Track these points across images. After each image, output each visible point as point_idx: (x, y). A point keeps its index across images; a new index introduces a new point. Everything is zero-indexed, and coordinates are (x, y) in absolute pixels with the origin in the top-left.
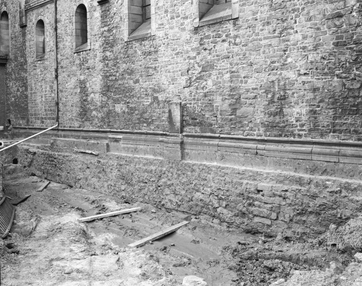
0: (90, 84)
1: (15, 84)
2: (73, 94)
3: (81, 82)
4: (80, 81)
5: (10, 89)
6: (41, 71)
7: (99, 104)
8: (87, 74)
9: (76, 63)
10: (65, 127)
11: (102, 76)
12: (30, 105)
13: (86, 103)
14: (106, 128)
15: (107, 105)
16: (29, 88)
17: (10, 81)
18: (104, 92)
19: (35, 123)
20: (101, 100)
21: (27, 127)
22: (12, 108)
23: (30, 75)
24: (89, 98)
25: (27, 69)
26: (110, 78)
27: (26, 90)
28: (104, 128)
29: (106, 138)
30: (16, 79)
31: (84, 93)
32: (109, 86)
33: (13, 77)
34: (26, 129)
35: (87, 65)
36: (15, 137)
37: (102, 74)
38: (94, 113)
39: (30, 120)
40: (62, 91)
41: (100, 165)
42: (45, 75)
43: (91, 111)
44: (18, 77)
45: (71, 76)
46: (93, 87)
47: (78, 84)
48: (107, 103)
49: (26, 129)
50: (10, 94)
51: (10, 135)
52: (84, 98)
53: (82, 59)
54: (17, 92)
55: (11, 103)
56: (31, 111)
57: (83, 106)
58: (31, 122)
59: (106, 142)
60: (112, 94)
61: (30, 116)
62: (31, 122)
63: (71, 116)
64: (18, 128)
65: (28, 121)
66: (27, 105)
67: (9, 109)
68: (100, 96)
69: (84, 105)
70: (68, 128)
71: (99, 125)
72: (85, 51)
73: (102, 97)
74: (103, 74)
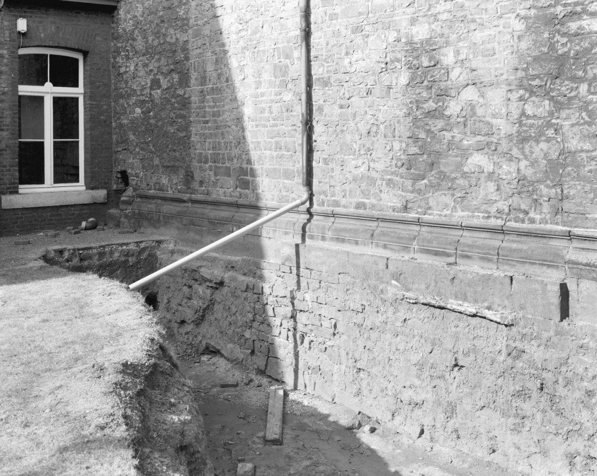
0: (457, 53)
1: (145, 65)
2: (377, 91)
3: (415, 49)
4: (410, 43)
5: (126, 82)
6: (240, 21)
7: (504, 127)
8: (445, 16)
10: (337, 204)
11: (525, 18)
12: (193, 130)
13: (440, 124)
14: (543, 221)
15: (550, 133)
16: (194, 75)
17: (128, 58)
18: (537, 82)
19: (215, 184)
20: (515, 114)
21: (186, 197)
22: (132, 137)
23: (197, 34)
24: (452, 104)
25: (188, 19)
26: (573, 26)
27: (185, 80)
28: (532, 221)
29: (550, 262)
30: (149, 52)
32: (565, 55)
33: (140, 44)
34: (184, 201)
36: (145, 223)
37: (523, 13)
38: (478, 160)
39: (197, 176)
40: (326, 83)
41: (519, 364)
42: (255, 32)
43: (465, 154)
44: (156, 43)
45: (367, 28)
46: (478, 62)
47: (399, 56)
48: (549, 125)
49: (184, 201)
50: (129, 96)
51: (126, 216)
52: (431, 105)
54: (151, 88)
55: (132, 122)
56: (200, 146)
57: (422, 135)
58: (201, 183)
59: (554, 277)
60: (584, 88)
61: (195, 164)
62: (201, 183)
63: (365, 167)
64: (153, 197)
65: (189, 177)
66: (186, 128)
67: (125, 141)
68: (515, 96)
69: (428, 132)
70: (352, 210)
71: (503, 205)
73: (521, 99)
74: (533, 12)
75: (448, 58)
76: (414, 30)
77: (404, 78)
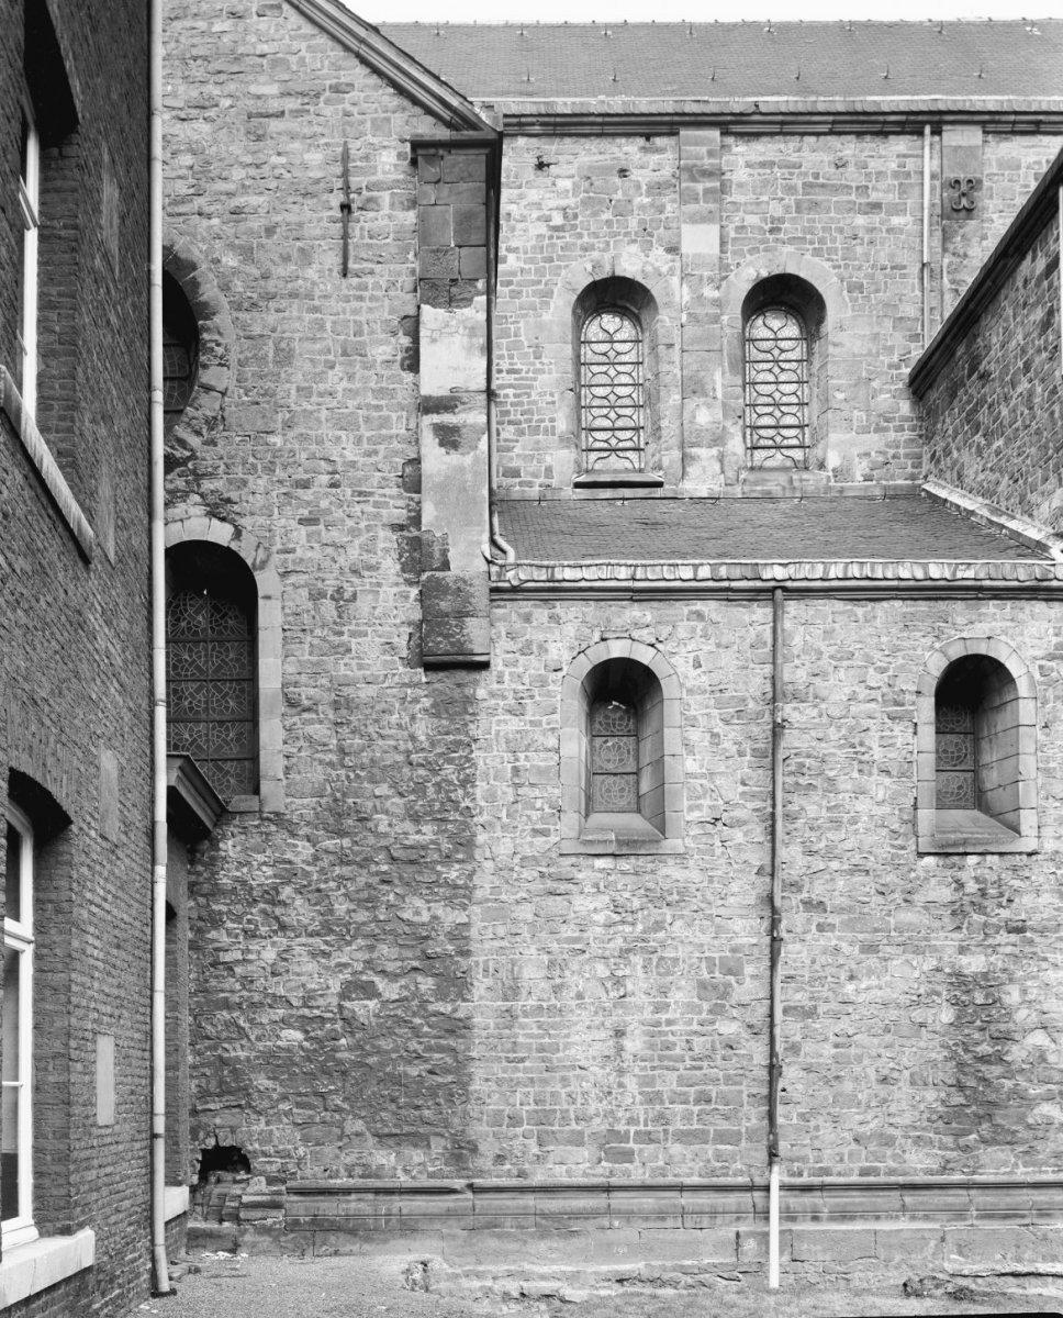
0: (1024, 992)
4: (959, 975)
9: (919, 898)
10: (826, 1172)
13: (997, 1070)
24: (1015, 1048)
31: (982, 1029)
35: (1005, 914)
47: (939, 988)
53: (972, 887)
57: (971, 1083)
70: (855, 1179)
72: (1001, 854)
75: (1012, 996)
76: (964, 960)
77: (947, 1015)
